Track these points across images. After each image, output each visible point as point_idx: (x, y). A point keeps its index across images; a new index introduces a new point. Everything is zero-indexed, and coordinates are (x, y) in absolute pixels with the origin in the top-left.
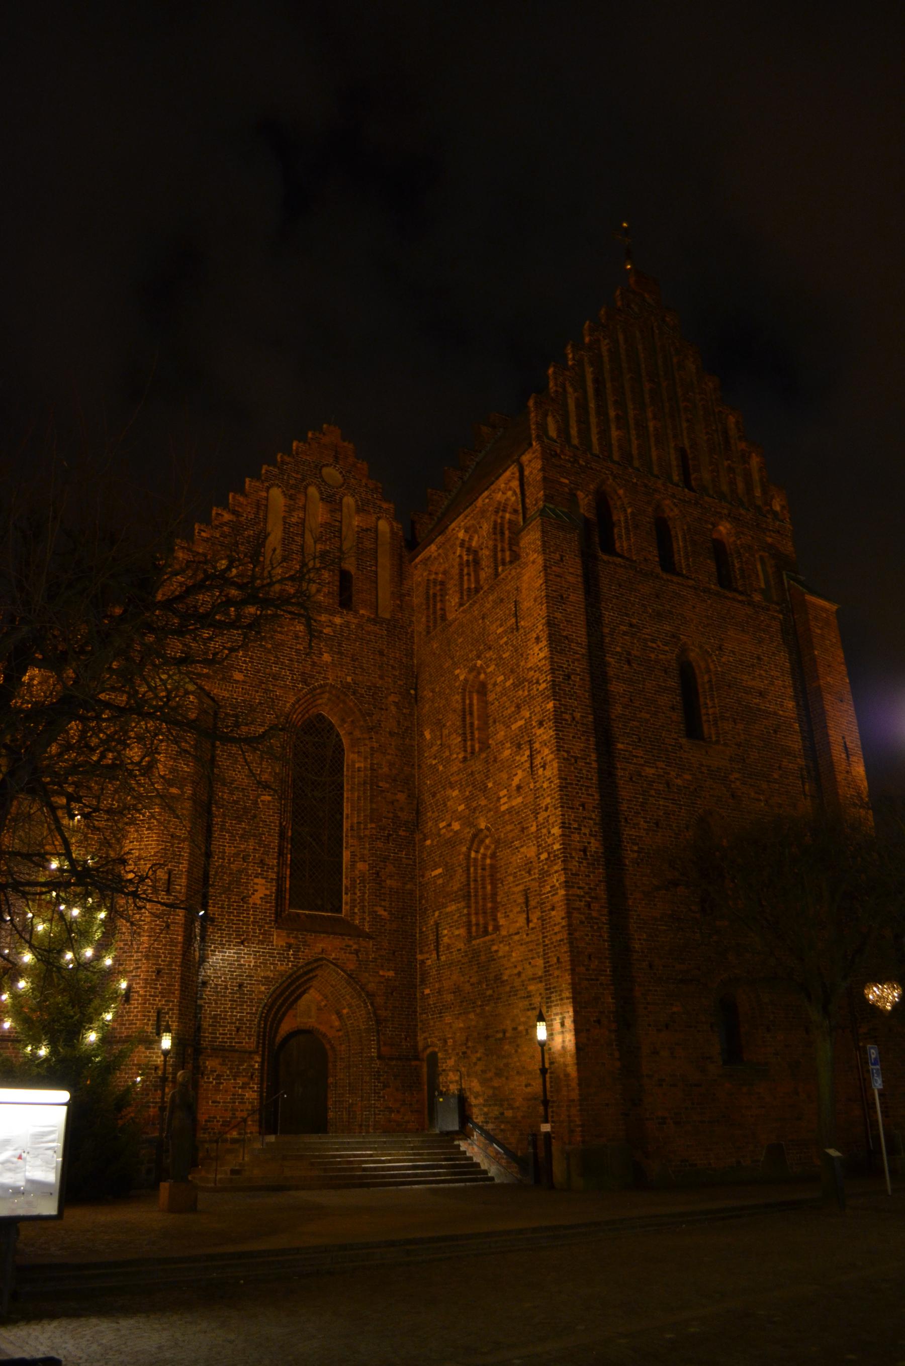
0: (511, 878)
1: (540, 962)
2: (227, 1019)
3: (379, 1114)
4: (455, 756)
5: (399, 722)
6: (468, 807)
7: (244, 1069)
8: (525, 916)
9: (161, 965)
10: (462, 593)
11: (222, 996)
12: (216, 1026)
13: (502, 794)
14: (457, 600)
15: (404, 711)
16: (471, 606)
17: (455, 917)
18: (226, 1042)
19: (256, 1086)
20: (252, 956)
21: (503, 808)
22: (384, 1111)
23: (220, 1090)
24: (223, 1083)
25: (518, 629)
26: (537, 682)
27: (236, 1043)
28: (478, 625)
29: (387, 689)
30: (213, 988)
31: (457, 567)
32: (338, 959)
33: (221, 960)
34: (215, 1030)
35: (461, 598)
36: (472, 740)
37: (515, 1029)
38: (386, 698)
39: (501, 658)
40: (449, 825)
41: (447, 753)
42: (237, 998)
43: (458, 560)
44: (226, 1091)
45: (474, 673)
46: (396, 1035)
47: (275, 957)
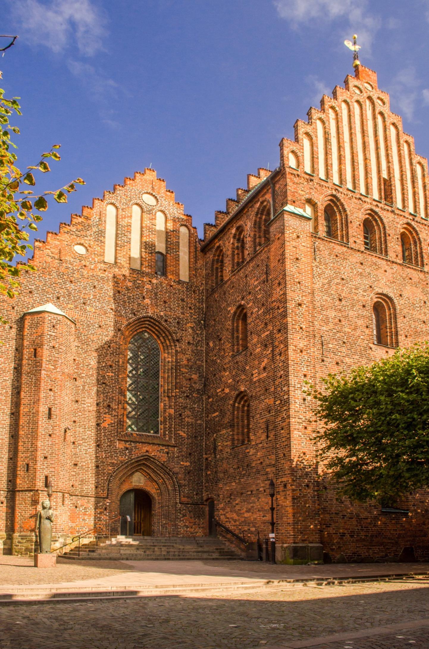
0: (258, 416)
1: (273, 457)
4: (227, 354)
6: (234, 380)
8: (266, 434)
10: (233, 265)
13: (254, 372)
14: (230, 269)
16: (239, 271)
17: (225, 437)
21: (255, 380)
25: (267, 281)
26: (278, 308)
28: (243, 281)
29: (187, 320)
31: (230, 249)
35: (233, 267)
36: (238, 345)
37: (258, 490)
39: (256, 298)
40: (223, 390)
41: (223, 353)
43: (231, 246)
45: (240, 309)
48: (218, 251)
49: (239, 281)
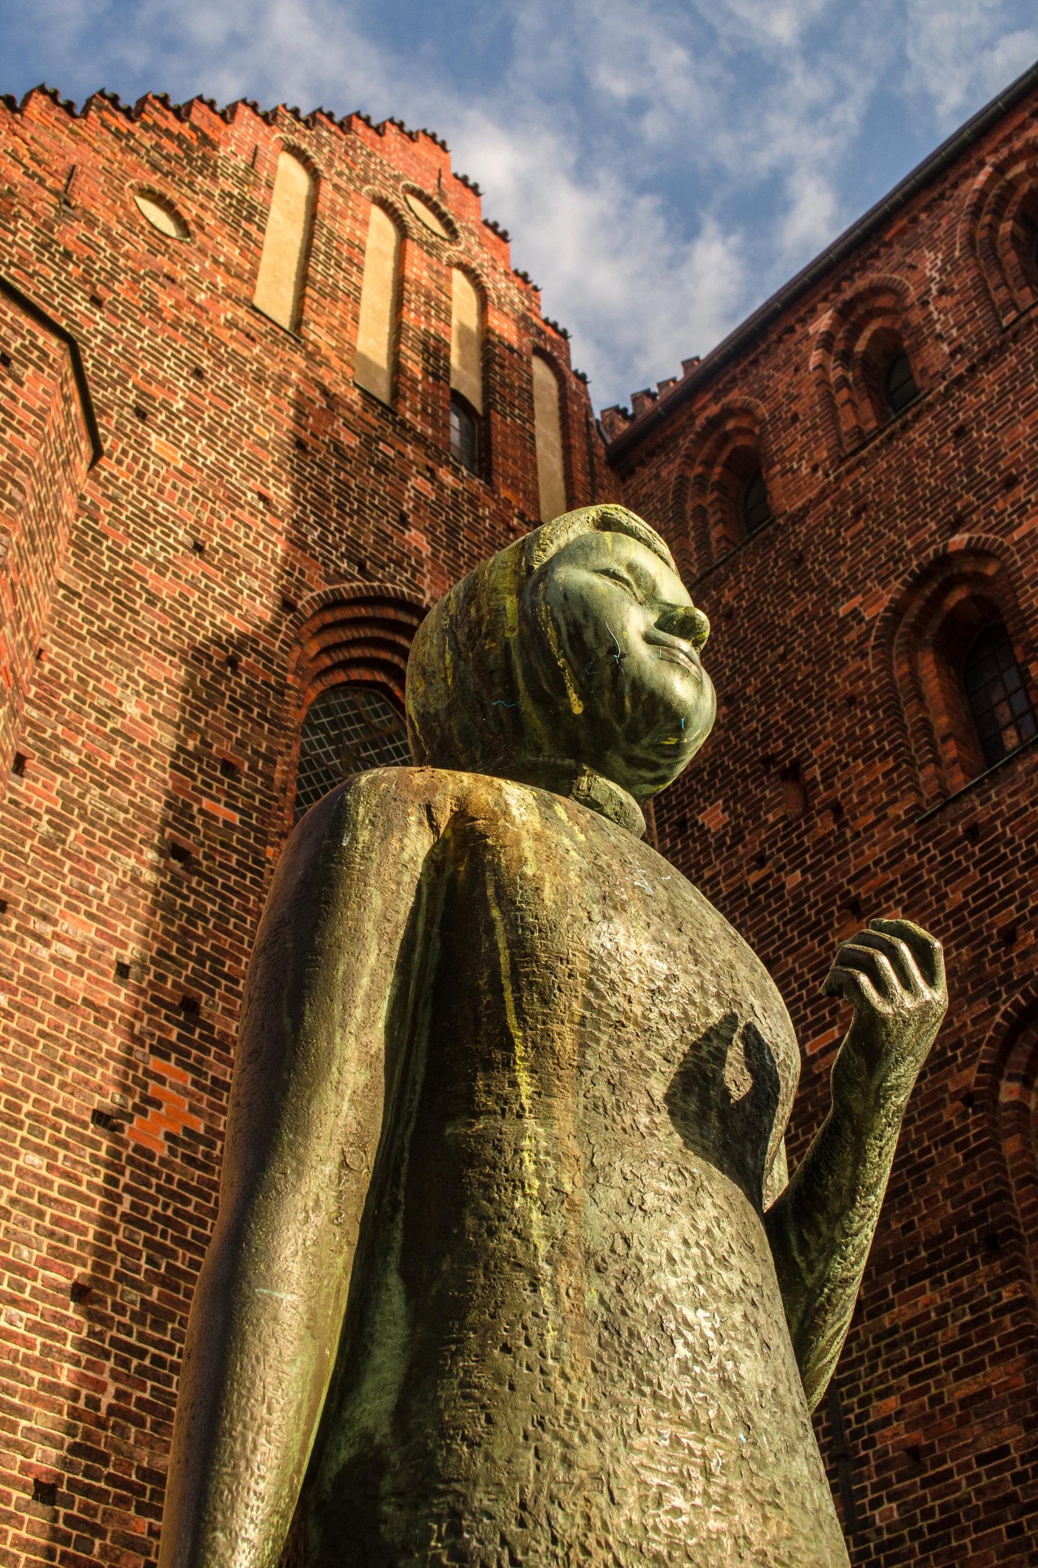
20: (110, 1364)
48: (709, 445)
49: (908, 473)
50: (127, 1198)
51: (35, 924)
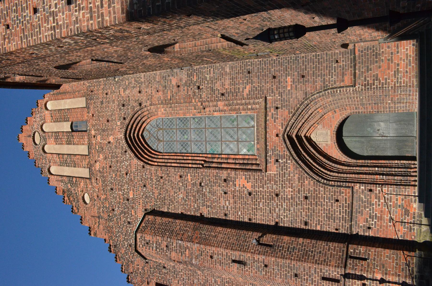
2: (329, 209)
3: (401, 82)
5: (134, 87)
7: (365, 198)
9: (291, 274)
11: (314, 212)
12: (335, 217)
15: (127, 84)
18: (346, 210)
19: (378, 189)
22: (398, 78)
23: (381, 216)
24: (376, 214)
27: (346, 203)
30: (309, 218)
32: (282, 123)
33: (289, 211)
34: (337, 218)
38: (123, 97)
42: (314, 201)
44: (382, 211)
46: (335, 72)
47: (285, 172)
50: (260, 189)
51: (226, 209)
